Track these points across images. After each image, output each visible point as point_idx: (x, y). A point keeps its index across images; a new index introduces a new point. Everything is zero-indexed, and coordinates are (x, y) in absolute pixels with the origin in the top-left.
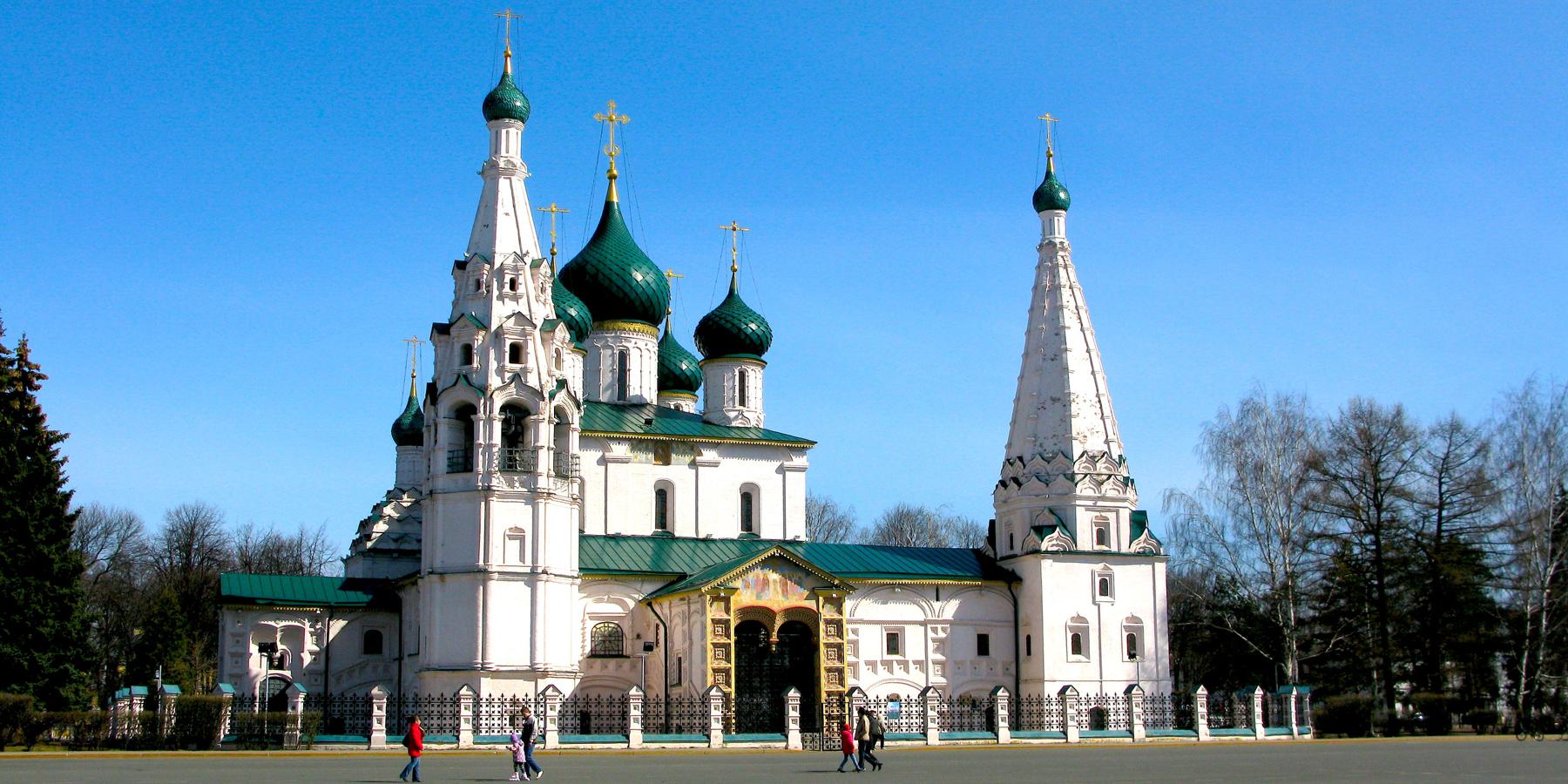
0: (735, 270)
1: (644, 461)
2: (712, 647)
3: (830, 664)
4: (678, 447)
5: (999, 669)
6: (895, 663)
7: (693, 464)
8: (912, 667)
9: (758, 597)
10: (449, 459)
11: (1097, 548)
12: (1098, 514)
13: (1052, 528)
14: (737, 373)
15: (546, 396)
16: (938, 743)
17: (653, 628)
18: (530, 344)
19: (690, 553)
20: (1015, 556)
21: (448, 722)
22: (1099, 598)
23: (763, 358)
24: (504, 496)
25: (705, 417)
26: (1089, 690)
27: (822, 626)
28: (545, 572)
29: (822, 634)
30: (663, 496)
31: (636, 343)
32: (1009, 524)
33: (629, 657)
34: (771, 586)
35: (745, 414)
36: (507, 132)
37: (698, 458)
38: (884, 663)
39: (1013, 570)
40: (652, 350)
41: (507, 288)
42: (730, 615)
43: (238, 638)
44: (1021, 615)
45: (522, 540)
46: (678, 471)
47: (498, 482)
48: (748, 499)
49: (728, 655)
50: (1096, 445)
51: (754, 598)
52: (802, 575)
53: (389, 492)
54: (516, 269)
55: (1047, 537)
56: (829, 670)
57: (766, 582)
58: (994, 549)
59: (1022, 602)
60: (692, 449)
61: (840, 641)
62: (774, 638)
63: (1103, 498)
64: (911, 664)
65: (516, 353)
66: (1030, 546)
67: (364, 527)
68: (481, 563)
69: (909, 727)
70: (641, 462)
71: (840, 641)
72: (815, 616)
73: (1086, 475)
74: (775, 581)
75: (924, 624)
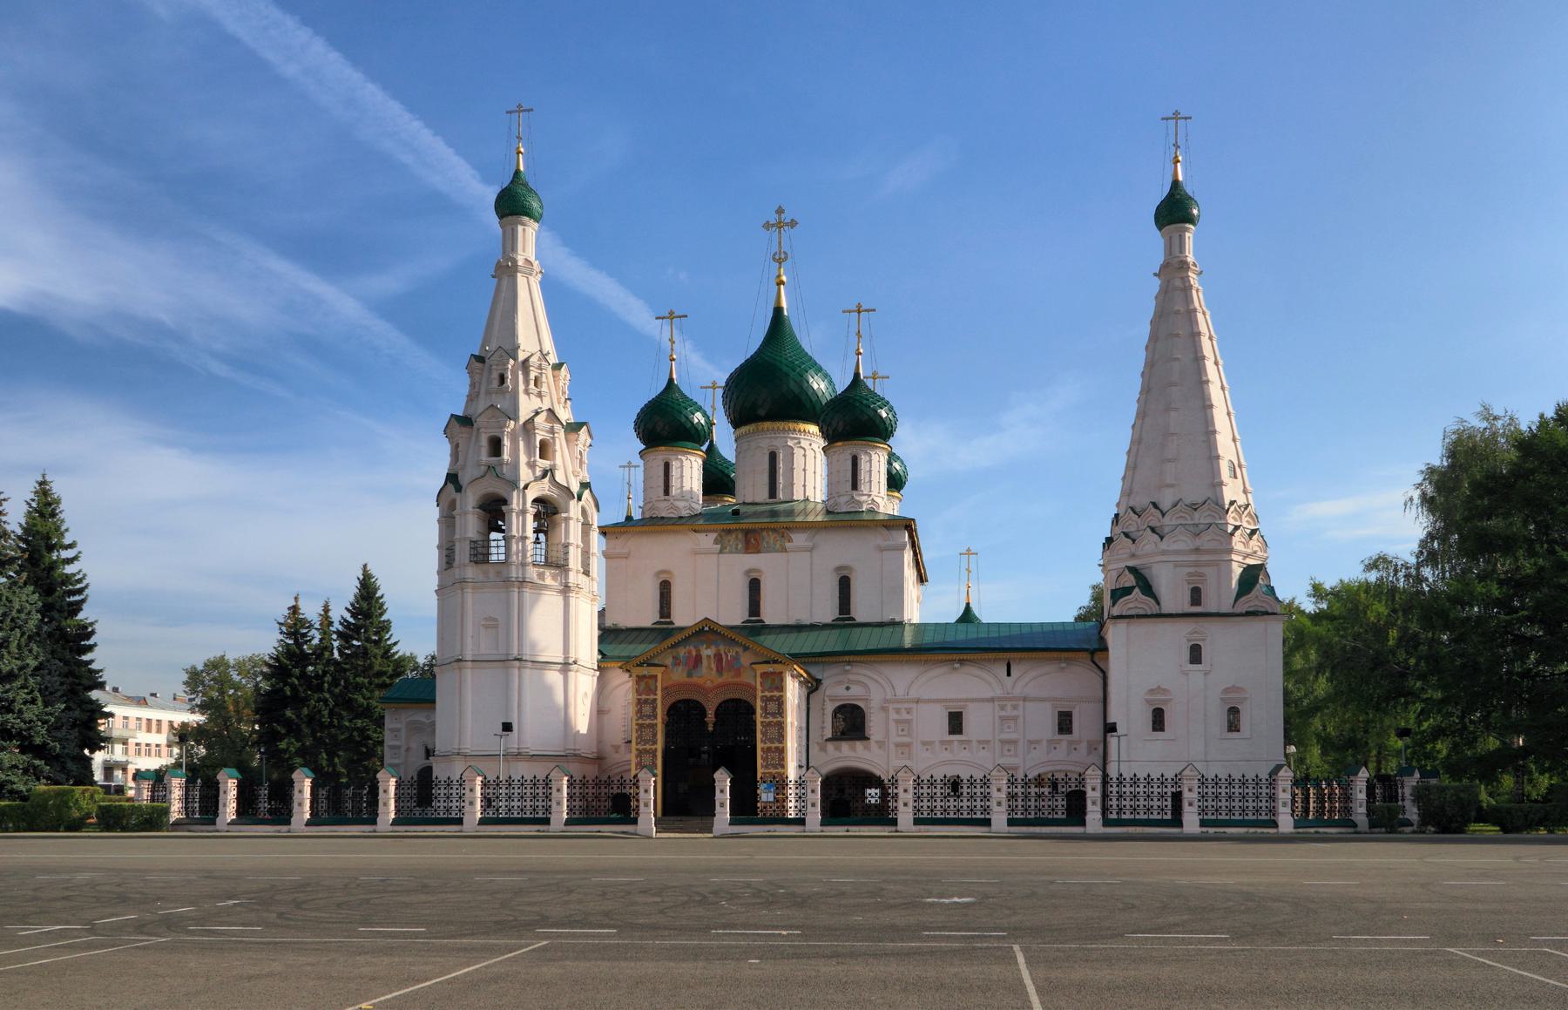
1: (734, 550)
3: (769, 745)
4: (769, 535)
5: (1083, 747)
6: (956, 743)
7: (784, 550)
9: (690, 675)
10: (446, 556)
13: (1127, 591)
14: (850, 458)
18: (557, 440)
27: (759, 704)
29: (759, 711)
30: (755, 586)
31: (810, 445)
35: (857, 498)
37: (788, 545)
38: (943, 742)
42: (656, 695)
43: (985, 746)
45: (496, 627)
48: (845, 585)
49: (655, 735)
51: (685, 674)
52: (740, 650)
54: (540, 367)
55: (1122, 600)
56: (769, 749)
57: (698, 659)
60: (783, 536)
62: (710, 716)
69: (534, 810)
70: (731, 552)
72: (755, 689)
74: (708, 657)
75: (992, 700)
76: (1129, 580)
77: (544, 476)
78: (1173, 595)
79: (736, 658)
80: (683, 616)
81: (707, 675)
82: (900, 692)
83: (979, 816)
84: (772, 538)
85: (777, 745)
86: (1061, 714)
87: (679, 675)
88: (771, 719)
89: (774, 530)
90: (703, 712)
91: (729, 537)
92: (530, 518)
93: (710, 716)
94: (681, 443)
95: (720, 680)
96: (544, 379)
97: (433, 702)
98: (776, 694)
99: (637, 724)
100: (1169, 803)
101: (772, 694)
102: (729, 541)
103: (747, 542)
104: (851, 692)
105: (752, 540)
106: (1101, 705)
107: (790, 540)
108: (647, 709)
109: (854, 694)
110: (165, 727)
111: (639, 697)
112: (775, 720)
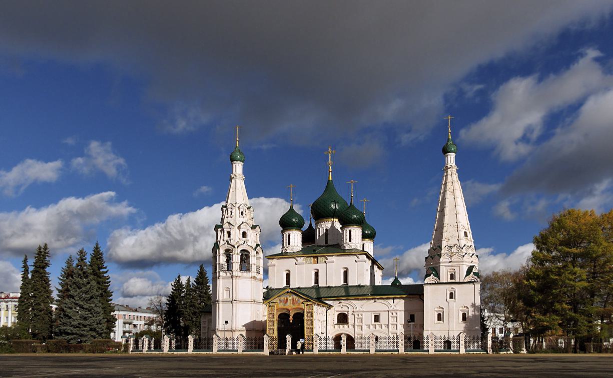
8: (383, 326)
9: (284, 305)
11: (449, 281)
15: (236, 246)
16: (317, 353)
24: (224, 278)
26: (444, 334)
27: (305, 314)
30: (317, 274)
46: (321, 266)
47: (222, 274)
48: (346, 274)
51: (283, 305)
56: (308, 328)
57: (287, 300)
62: (291, 318)
63: (450, 262)
64: (390, 326)
65: (229, 233)
68: (218, 298)
74: (290, 300)
76: (430, 271)
78: (445, 276)
79: (298, 300)
80: (293, 285)
81: (290, 306)
82: (358, 309)
83: (366, 349)
86: (410, 315)
87: (281, 305)
89: (322, 256)
90: (288, 315)
92: (239, 257)
93: (291, 318)
95: (294, 307)
97: (211, 312)
100: (443, 345)
103: (314, 260)
104: (343, 309)
107: (327, 259)
108: (272, 316)
109: (344, 310)
110: (142, 318)
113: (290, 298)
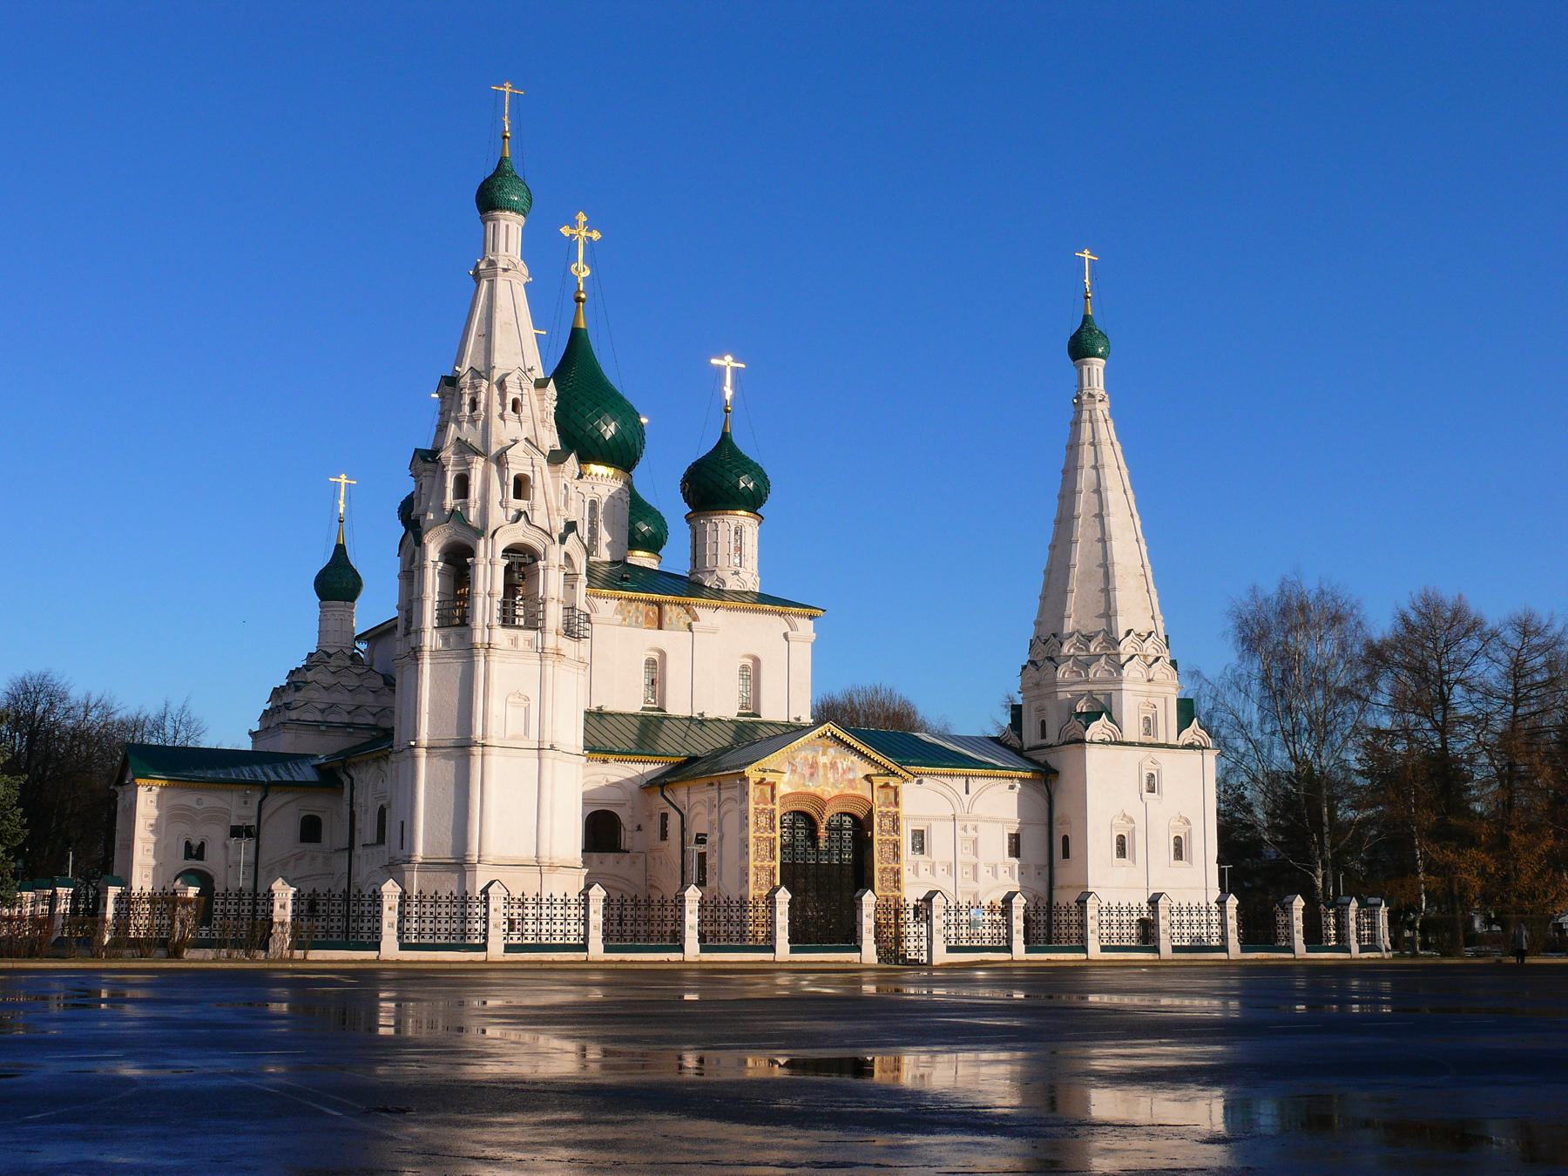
0: (727, 411)
1: (634, 624)
2: (754, 840)
3: (885, 865)
4: (671, 610)
11: (1144, 739)
12: (1144, 699)
17: (657, 819)
19: (685, 729)
20: (1051, 746)
21: (642, 929)
22: (1145, 794)
23: (758, 511)
25: (693, 578)
27: (876, 820)
28: (552, 747)
32: (1041, 710)
33: (628, 852)
34: (821, 772)
36: (507, 226)
39: (1046, 762)
40: (625, 501)
41: (509, 407)
42: (774, 804)
44: (1056, 815)
46: (671, 640)
47: (501, 636)
49: (772, 850)
50: (1143, 626)
53: (311, 655)
58: (1020, 737)
59: (1056, 799)
61: (896, 837)
65: (521, 487)
66: (1072, 734)
67: (280, 696)
70: (629, 626)
71: (896, 837)
73: (1132, 658)
77: (517, 519)
84: (675, 614)
85: (893, 865)
88: (887, 837)
91: (629, 608)
94: (717, 512)
96: (525, 401)
98: (893, 809)
99: (754, 837)
101: (888, 809)
102: (629, 612)
105: (651, 613)
106: (1045, 830)
107: (696, 619)
111: (756, 806)
112: (891, 838)
113: (823, 760)
